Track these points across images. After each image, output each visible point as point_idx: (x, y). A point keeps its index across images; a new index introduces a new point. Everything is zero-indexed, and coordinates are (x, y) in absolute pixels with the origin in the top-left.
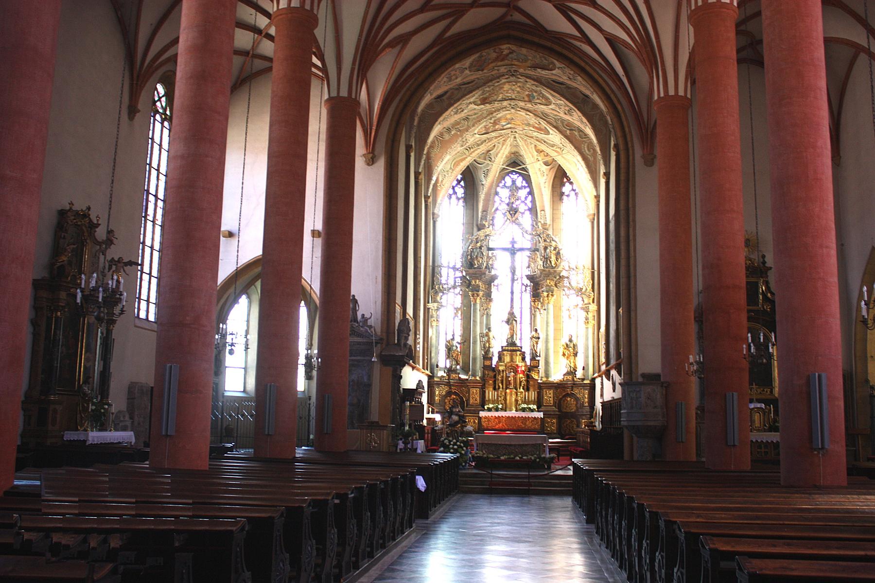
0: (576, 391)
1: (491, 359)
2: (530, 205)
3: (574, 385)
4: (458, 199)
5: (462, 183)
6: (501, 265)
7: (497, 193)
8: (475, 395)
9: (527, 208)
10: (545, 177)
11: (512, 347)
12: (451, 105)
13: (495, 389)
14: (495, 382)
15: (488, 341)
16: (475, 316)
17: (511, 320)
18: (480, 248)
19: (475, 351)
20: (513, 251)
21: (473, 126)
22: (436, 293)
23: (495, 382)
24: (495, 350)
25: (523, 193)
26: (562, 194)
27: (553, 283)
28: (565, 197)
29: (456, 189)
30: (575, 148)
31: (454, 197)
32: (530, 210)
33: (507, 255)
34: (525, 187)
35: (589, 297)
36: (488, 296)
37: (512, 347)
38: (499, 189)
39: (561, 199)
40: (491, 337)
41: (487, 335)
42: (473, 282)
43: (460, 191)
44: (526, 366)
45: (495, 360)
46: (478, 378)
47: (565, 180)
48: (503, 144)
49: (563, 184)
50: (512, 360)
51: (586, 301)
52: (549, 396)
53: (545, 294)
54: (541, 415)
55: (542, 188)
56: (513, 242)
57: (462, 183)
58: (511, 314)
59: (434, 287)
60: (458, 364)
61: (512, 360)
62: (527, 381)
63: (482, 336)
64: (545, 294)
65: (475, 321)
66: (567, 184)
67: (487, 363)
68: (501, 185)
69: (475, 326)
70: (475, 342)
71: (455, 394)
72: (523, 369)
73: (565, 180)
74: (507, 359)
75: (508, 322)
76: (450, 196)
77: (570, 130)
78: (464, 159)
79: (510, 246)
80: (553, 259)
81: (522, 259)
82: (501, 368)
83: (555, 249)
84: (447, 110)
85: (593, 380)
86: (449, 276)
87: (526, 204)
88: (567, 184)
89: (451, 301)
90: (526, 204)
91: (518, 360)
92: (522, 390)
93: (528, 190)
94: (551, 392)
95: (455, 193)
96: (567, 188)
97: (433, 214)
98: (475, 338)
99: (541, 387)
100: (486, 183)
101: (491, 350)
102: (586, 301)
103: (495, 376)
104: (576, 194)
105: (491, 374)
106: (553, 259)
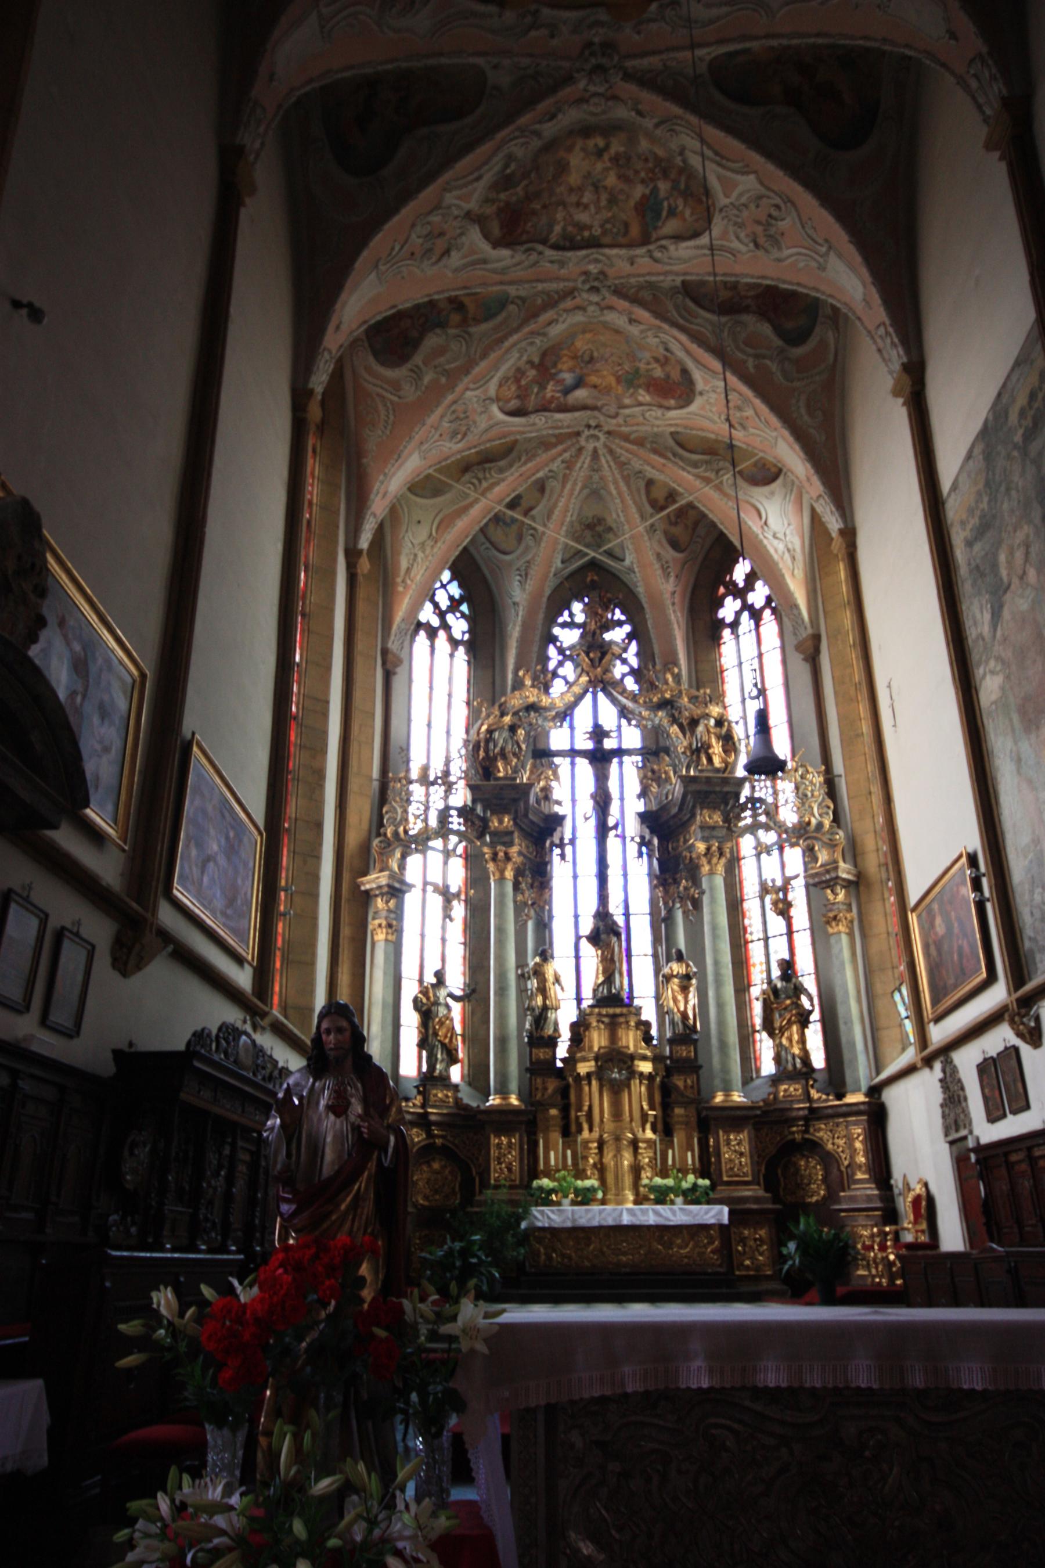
0: (822, 1133)
1: (552, 1042)
2: (634, 662)
3: (815, 1114)
4: (454, 643)
5: (464, 608)
6: (570, 789)
7: (554, 639)
8: (504, 1152)
9: (626, 669)
10: (672, 579)
11: (612, 1003)
12: (406, 196)
13: (566, 1133)
14: (565, 1110)
15: (543, 990)
16: (501, 915)
17: (606, 933)
18: (513, 729)
19: (502, 1017)
20: (600, 758)
21: (484, 356)
22: (388, 846)
23: (565, 1110)
24: (565, 1016)
25: (617, 635)
26: (721, 624)
27: (717, 818)
28: (727, 633)
29: (450, 618)
30: (774, 408)
31: (442, 634)
32: (633, 672)
33: (585, 768)
34: (620, 623)
35: (832, 845)
36: (537, 875)
37: (612, 1003)
38: (556, 631)
39: (716, 640)
40: (550, 978)
41: (538, 973)
42: (495, 823)
43: (459, 627)
44: (656, 1059)
45: (562, 1051)
46: (514, 1100)
47: (722, 590)
48: (566, 478)
49: (721, 605)
50: (613, 1037)
51: (823, 856)
52: (736, 1149)
53: (701, 847)
54: (717, 1214)
55: (669, 602)
56: (598, 733)
57: (464, 608)
58: (603, 915)
59: (380, 838)
60: (453, 1059)
61: (613, 1037)
62: (666, 1107)
63: (522, 978)
64: (701, 847)
65: (501, 930)
66: (729, 600)
67: (542, 1054)
68: (560, 620)
69: (501, 943)
70: (502, 991)
71: (445, 1152)
72: (646, 1067)
73: (722, 590)
74: (598, 1040)
75: (595, 938)
76: (432, 633)
77: (757, 356)
78: (465, 509)
79: (589, 745)
80: (717, 748)
81: (627, 778)
82: (583, 1068)
83: (720, 723)
84: (396, 210)
85: (875, 1091)
86: (422, 806)
87: (624, 662)
88: (729, 600)
89: (432, 874)
90: (624, 662)
91: (630, 1040)
92: (649, 1134)
93: (627, 628)
94: (743, 1136)
95: (446, 626)
96: (729, 608)
97: (385, 652)
98: (501, 977)
99: (710, 1121)
100: (519, 596)
101: (551, 1015)
102: (823, 856)
103: (565, 1092)
104: (756, 615)
105: (552, 1085)
106: (717, 748)
